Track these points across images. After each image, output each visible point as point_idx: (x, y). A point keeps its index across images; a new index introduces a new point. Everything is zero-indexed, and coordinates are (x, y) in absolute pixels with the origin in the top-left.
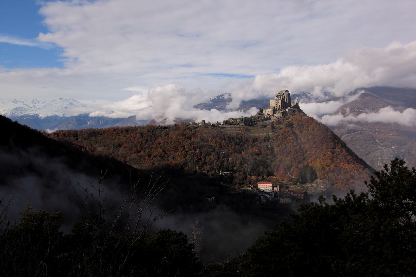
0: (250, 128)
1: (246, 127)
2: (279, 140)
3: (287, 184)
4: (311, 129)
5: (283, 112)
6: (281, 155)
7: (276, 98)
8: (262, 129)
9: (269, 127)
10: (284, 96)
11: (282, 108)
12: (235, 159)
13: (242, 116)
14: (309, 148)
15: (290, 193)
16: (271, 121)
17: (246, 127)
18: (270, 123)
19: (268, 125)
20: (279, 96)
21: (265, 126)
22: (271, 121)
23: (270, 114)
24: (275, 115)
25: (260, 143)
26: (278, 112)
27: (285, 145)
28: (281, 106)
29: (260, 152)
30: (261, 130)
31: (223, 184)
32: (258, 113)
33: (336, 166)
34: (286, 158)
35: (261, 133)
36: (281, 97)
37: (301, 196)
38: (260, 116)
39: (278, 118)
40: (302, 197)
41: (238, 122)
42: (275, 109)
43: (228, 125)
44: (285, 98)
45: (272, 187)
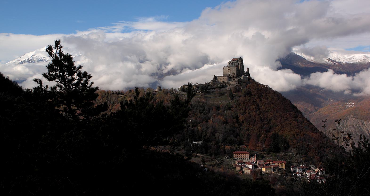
0: (208, 96)
1: (205, 94)
2: (242, 108)
3: (261, 154)
4: (271, 98)
5: (239, 80)
6: (247, 124)
7: (229, 65)
8: (220, 97)
9: (226, 94)
10: (238, 63)
11: (236, 76)
12: (204, 127)
13: (197, 83)
14: (273, 117)
15: (269, 162)
16: (228, 88)
17: (205, 94)
18: (228, 91)
19: (226, 93)
20: (233, 63)
21: (223, 94)
22: (228, 88)
23: (226, 81)
24: (230, 82)
25: (224, 111)
26: (232, 80)
27: (249, 113)
28: (235, 74)
29: (226, 120)
30: (219, 97)
31: (198, 155)
32: (212, 81)
33: (305, 135)
34: (253, 127)
35: (220, 101)
36: (235, 65)
37: (281, 165)
38: (214, 83)
39: (234, 86)
40: (281, 166)
41: (194, 89)
42: (230, 77)
43: (184, 92)
44: (239, 66)
45: (249, 157)
